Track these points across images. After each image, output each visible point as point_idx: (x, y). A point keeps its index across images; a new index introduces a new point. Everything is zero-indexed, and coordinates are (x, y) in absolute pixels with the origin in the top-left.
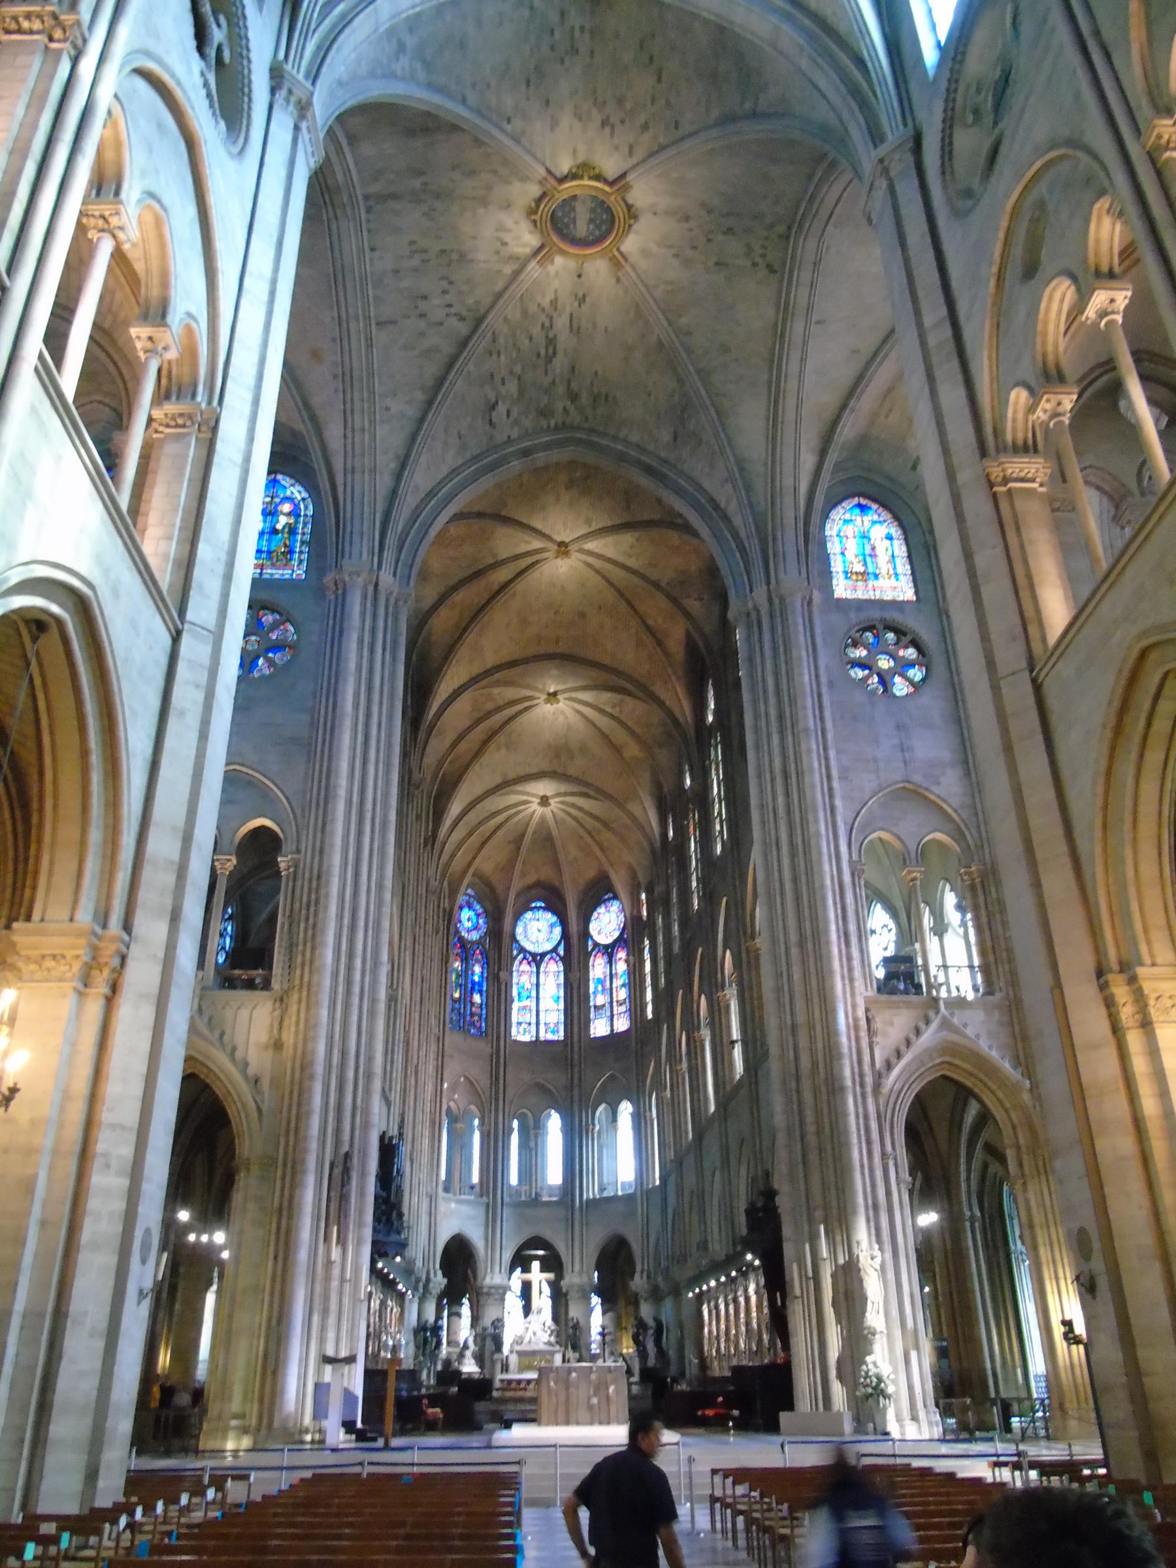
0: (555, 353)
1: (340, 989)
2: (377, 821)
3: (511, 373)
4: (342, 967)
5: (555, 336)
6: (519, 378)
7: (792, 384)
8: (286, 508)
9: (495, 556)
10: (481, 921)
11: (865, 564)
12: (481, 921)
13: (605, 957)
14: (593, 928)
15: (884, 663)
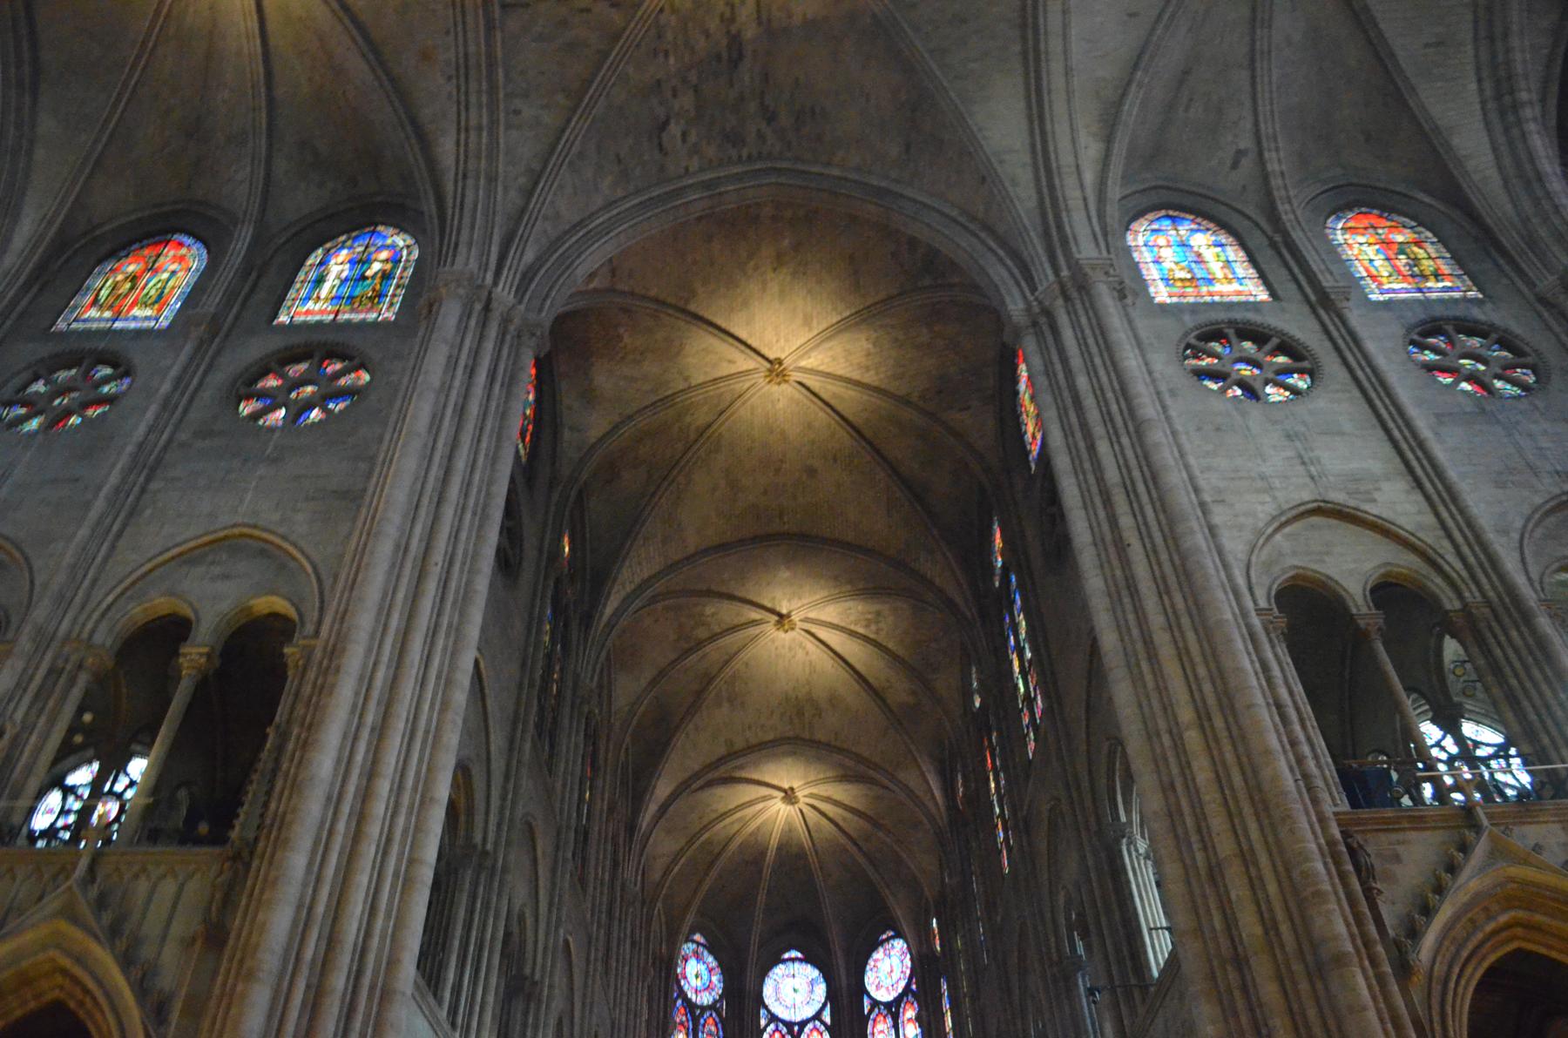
0: (741, 56)
1: (341, 826)
2: (453, 585)
3: (684, 80)
4: (351, 789)
5: (739, 32)
6: (696, 90)
7: (1055, 45)
8: (384, 255)
9: (686, 379)
10: (714, 979)
11: (1191, 271)
12: (714, 979)
13: (889, 1020)
14: (870, 980)
15: (1246, 371)
